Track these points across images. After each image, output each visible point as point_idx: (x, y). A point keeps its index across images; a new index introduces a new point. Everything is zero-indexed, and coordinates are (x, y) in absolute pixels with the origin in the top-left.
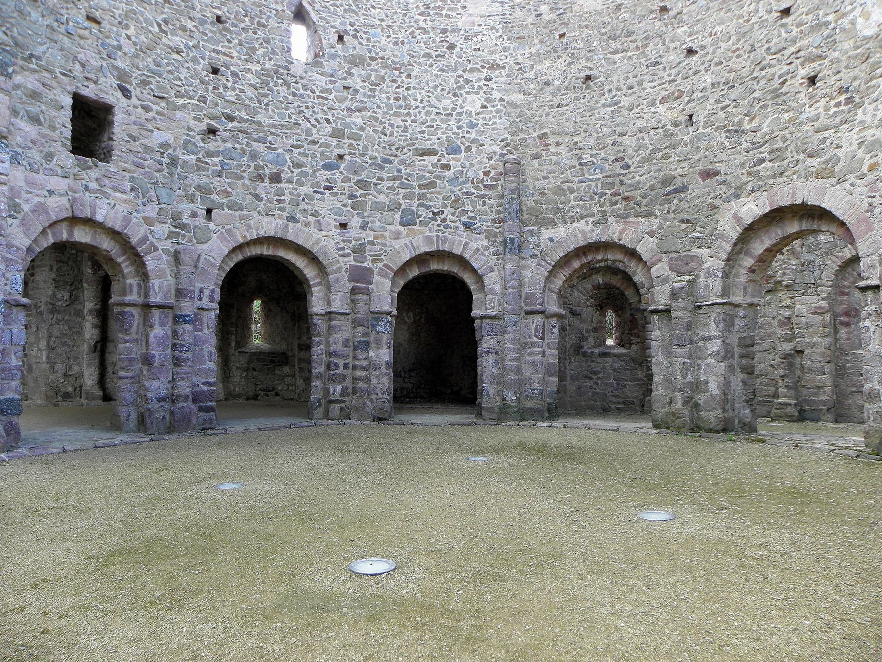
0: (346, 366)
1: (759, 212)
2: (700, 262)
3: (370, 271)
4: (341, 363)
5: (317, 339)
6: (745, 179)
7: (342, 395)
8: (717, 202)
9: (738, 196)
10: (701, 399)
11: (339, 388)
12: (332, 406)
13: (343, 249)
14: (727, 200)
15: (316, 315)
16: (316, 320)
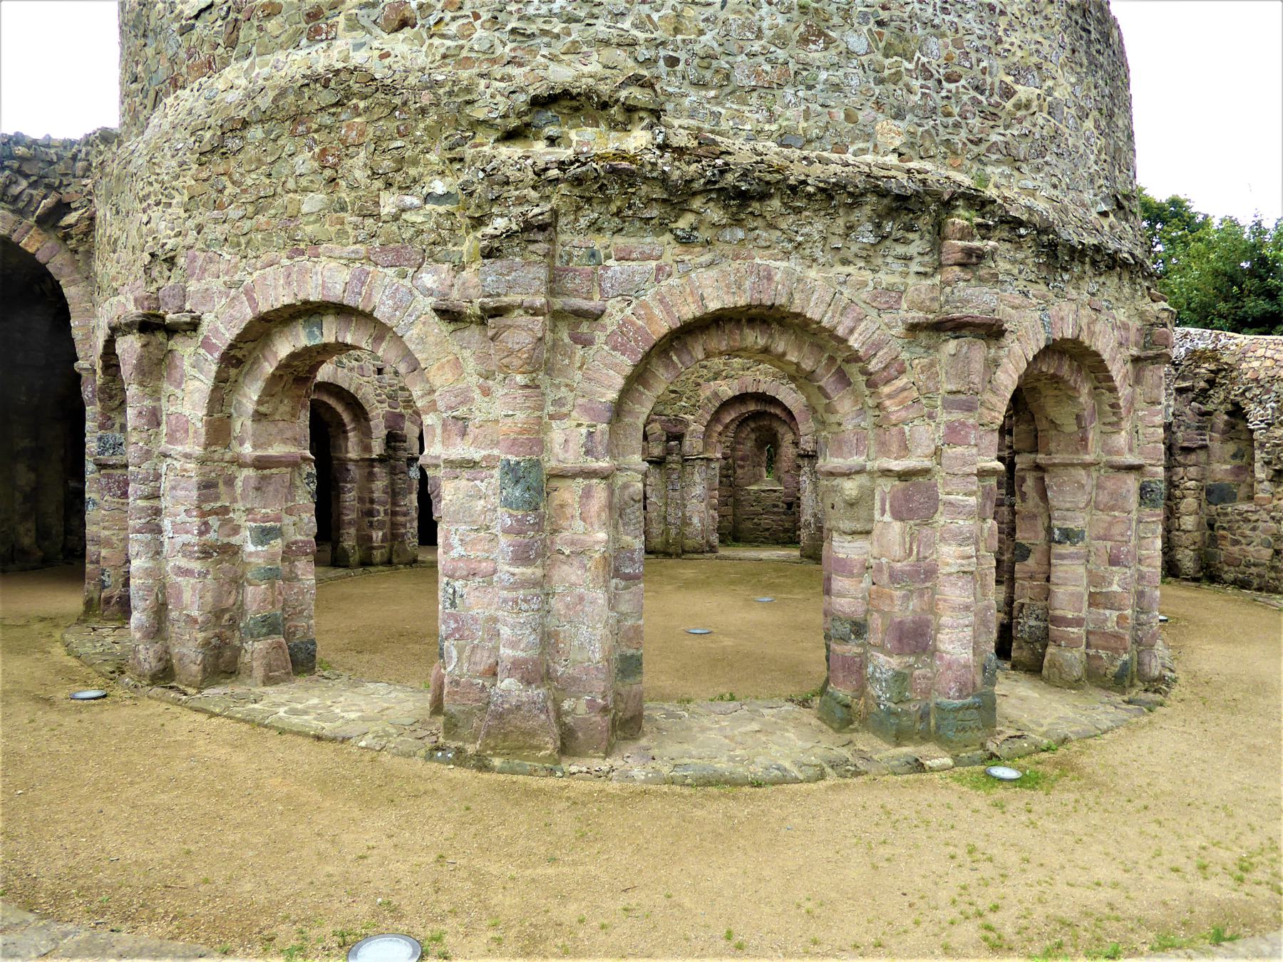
0: (386, 512)
1: (731, 393)
2: (687, 424)
3: (402, 416)
4: (382, 509)
5: (349, 486)
6: (722, 367)
7: (382, 541)
8: (701, 381)
9: (715, 379)
10: (688, 530)
11: (380, 534)
12: (375, 552)
13: (379, 395)
14: (708, 380)
15: (351, 460)
16: (351, 466)
